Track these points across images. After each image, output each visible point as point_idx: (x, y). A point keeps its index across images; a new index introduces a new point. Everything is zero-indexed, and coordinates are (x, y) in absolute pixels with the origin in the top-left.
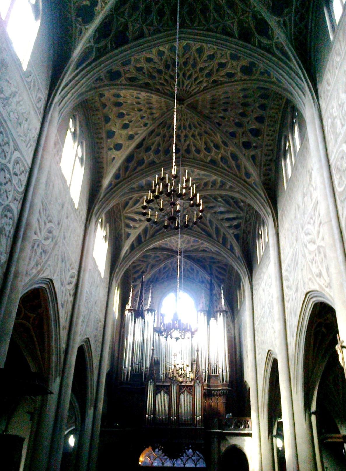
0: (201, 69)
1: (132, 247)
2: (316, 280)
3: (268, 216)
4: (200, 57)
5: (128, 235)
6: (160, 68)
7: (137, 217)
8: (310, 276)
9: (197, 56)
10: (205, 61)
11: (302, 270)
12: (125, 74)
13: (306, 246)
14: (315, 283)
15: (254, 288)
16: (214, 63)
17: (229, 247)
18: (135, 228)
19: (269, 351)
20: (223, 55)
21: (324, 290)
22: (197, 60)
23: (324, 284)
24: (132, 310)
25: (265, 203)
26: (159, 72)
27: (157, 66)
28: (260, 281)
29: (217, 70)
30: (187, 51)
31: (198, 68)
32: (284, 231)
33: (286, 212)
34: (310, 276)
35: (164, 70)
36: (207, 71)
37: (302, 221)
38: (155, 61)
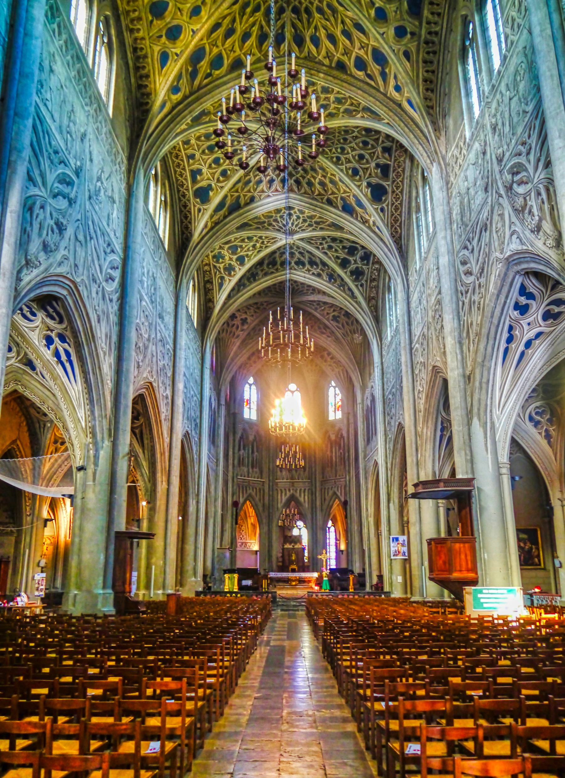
0: (257, 9)
4: (261, 27)
6: (319, 16)
9: (266, 28)
10: (254, 24)
12: (368, 45)
16: (240, 29)
20: (231, 51)
22: (264, 20)
26: (320, 10)
27: (323, 21)
29: (234, 20)
30: (280, 31)
31: (262, 9)
35: (315, 11)
36: (249, 10)
38: (324, 31)
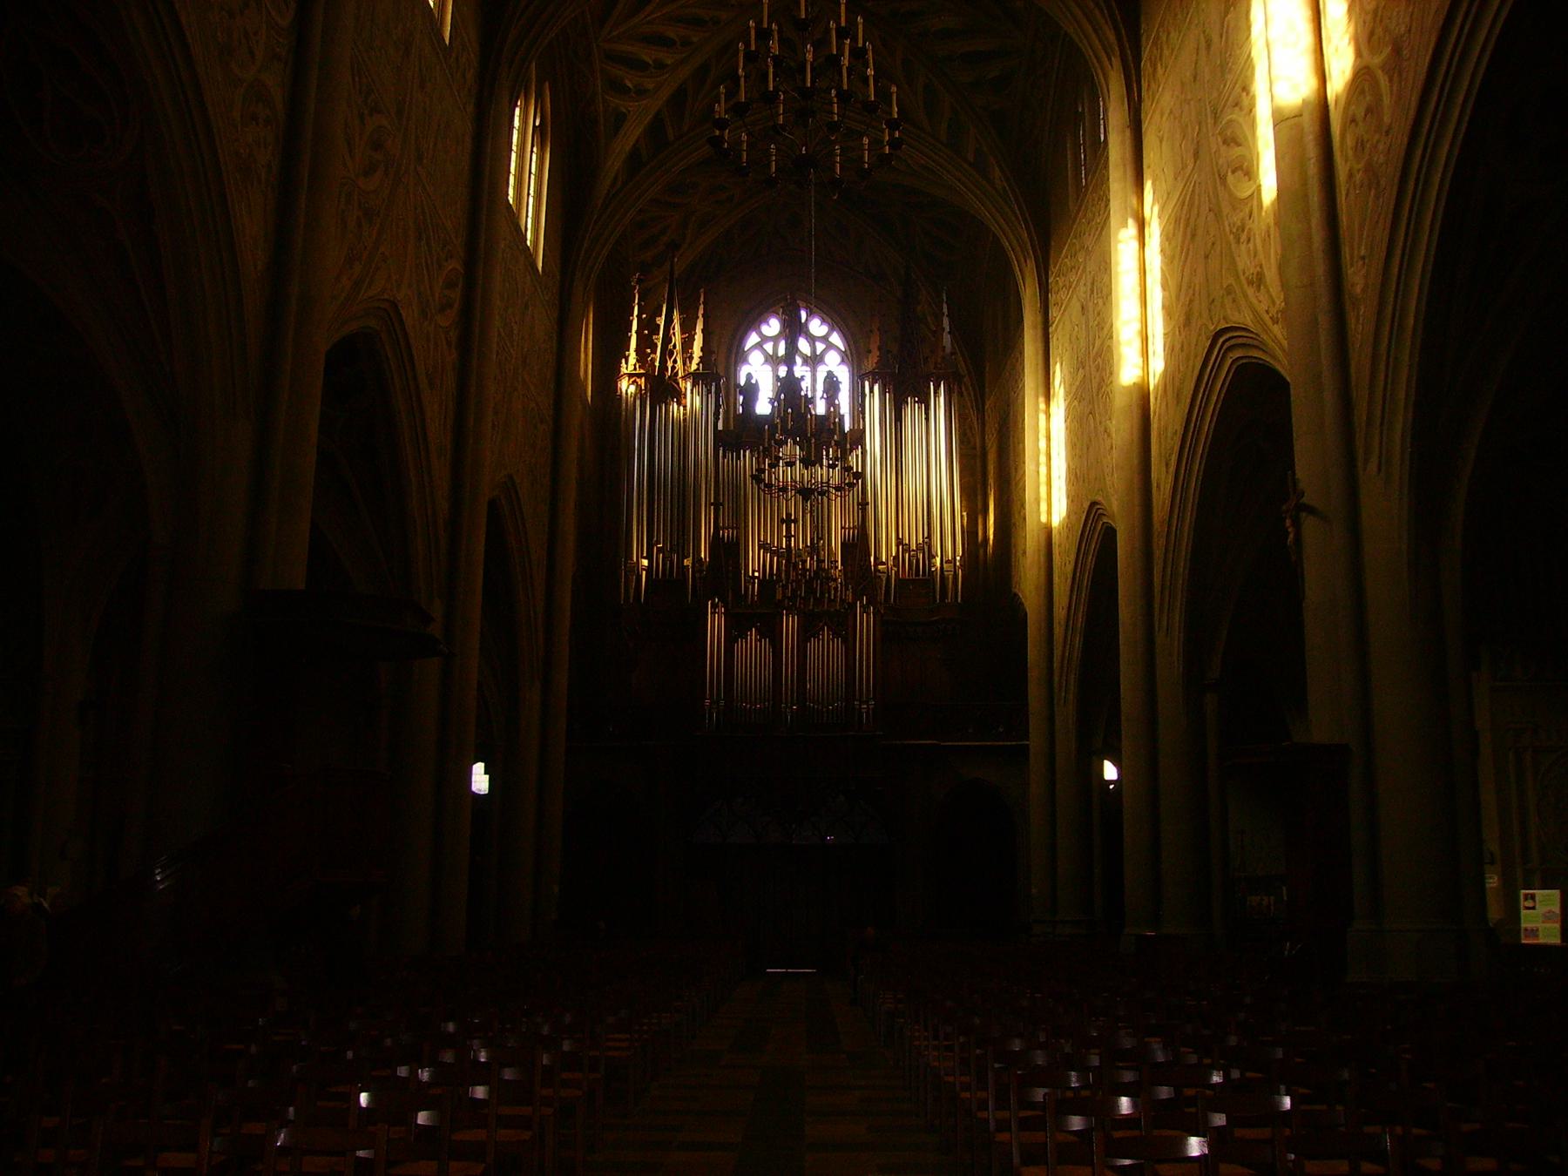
1: (635, 161)
2: (1246, 296)
3: (1110, 60)
5: (620, 119)
7: (647, 55)
8: (1231, 281)
11: (1207, 257)
13: (1223, 179)
14: (1242, 302)
15: (1052, 298)
17: (971, 158)
18: (641, 92)
19: (1093, 504)
21: (1267, 330)
23: (1267, 312)
24: (639, 376)
25: (1097, 12)
28: (1073, 277)
32: (1157, 116)
33: (1166, 52)
34: (1231, 281)
37: (1215, 94)
